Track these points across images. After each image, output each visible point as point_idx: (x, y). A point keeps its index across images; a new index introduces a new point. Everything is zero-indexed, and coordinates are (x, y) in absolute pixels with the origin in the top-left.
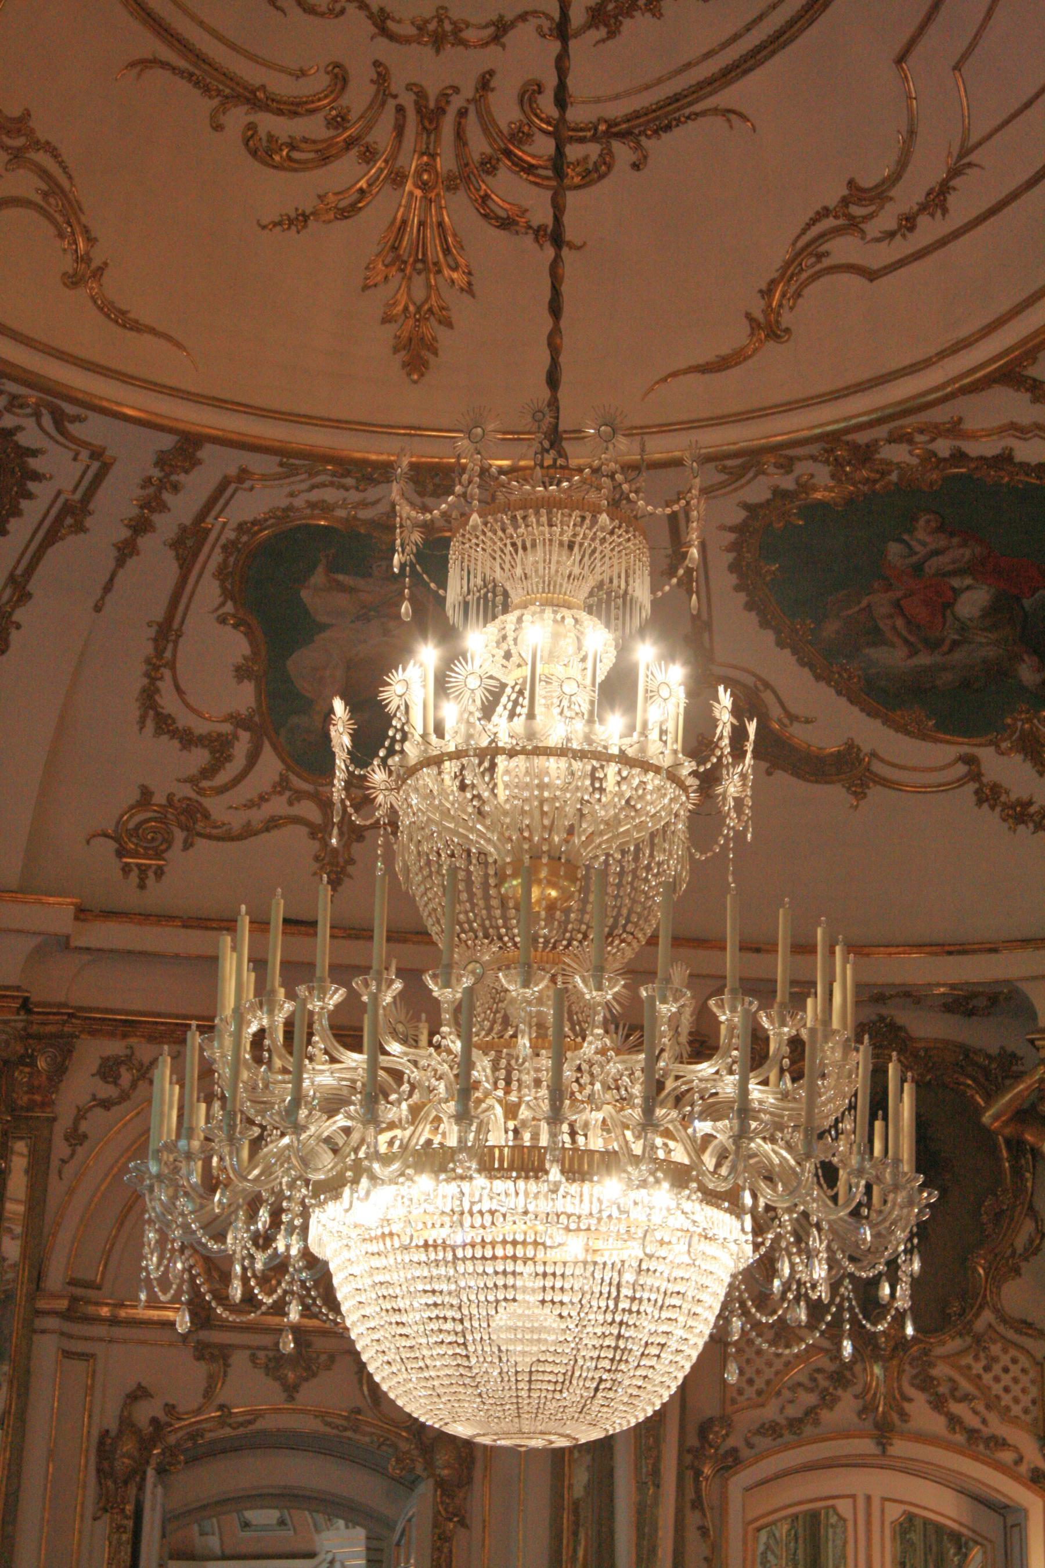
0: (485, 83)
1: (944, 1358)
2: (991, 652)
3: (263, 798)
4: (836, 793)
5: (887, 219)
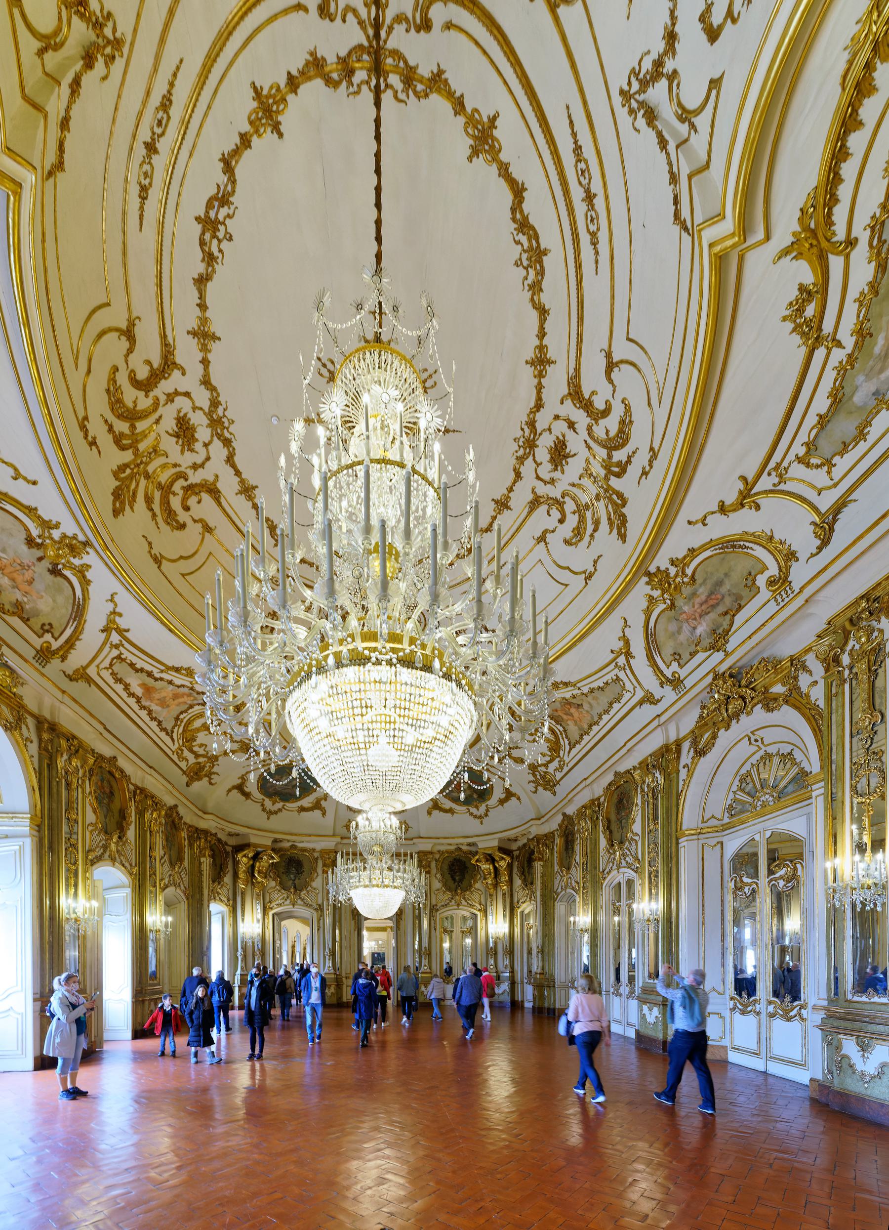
4: (449, 815)
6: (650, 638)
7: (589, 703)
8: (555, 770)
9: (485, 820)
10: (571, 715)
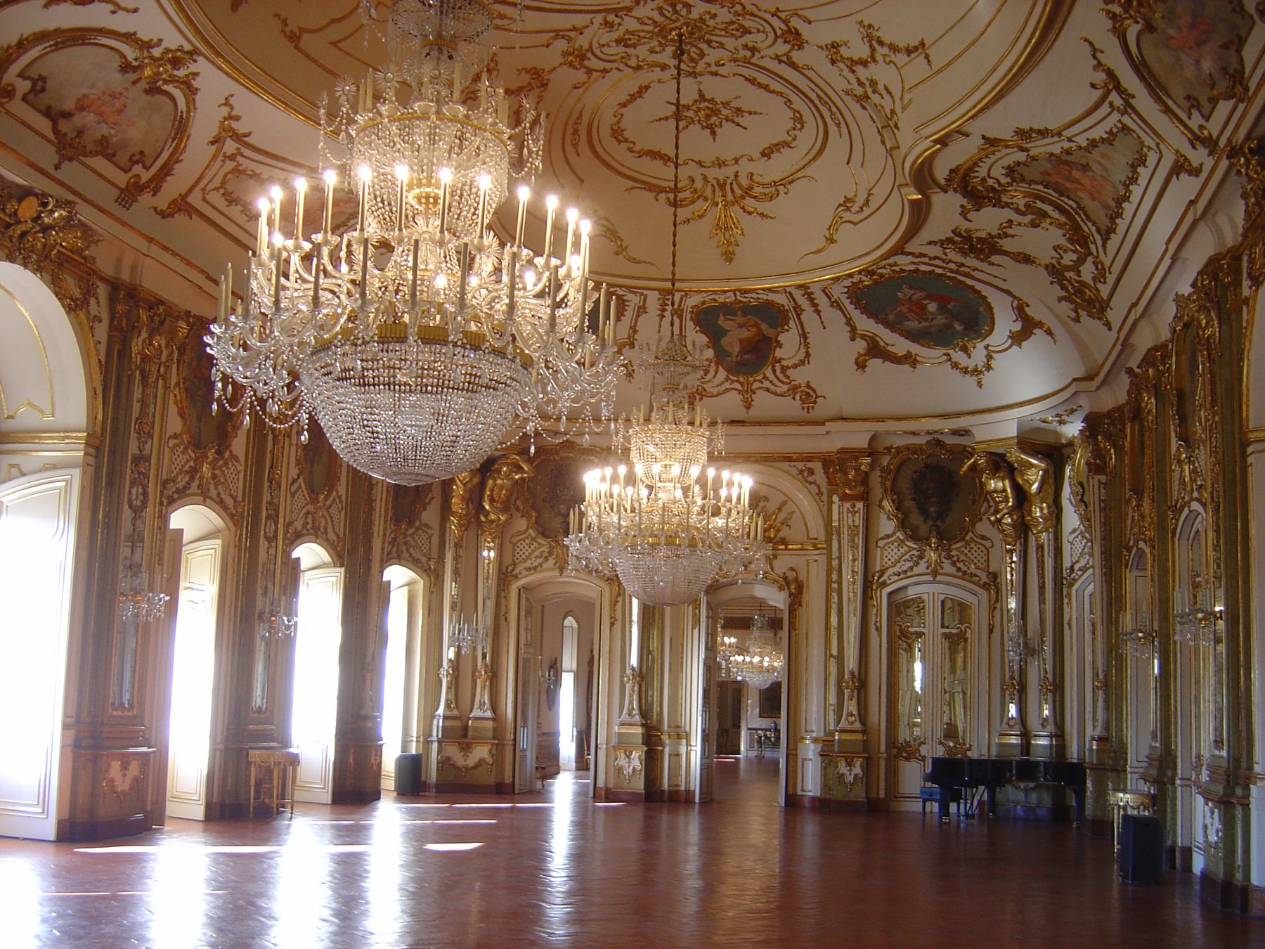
0: (736, 176)
1: (956, 549)
2: (944, 321)
3: (723, 383)
4: (907, 367)
5: (855, 208)
6: (1141, 68)
7: (1100, 164)
8: (1094, 279)
9: (987, 378)
10: (1078, 181)
